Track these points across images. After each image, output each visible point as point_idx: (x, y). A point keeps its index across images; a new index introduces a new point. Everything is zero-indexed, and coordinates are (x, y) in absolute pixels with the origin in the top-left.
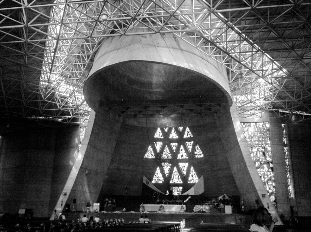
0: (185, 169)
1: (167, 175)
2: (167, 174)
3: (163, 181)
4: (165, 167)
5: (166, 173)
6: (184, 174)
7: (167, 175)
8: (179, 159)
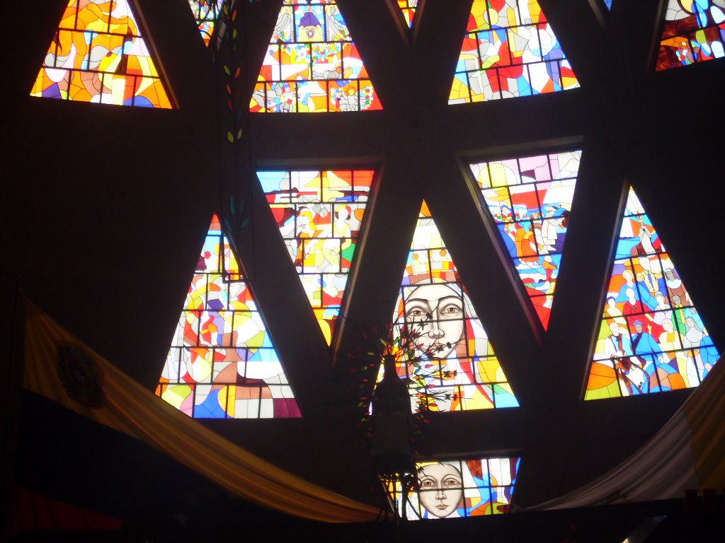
0: (551, 232)
1: (325, 318)
2: (332, 313)
3: (288, 393)
4: (305, 223)
5: (315, 301)
6: (529, 298)
7: (334, 324)
8: (472, 110)
